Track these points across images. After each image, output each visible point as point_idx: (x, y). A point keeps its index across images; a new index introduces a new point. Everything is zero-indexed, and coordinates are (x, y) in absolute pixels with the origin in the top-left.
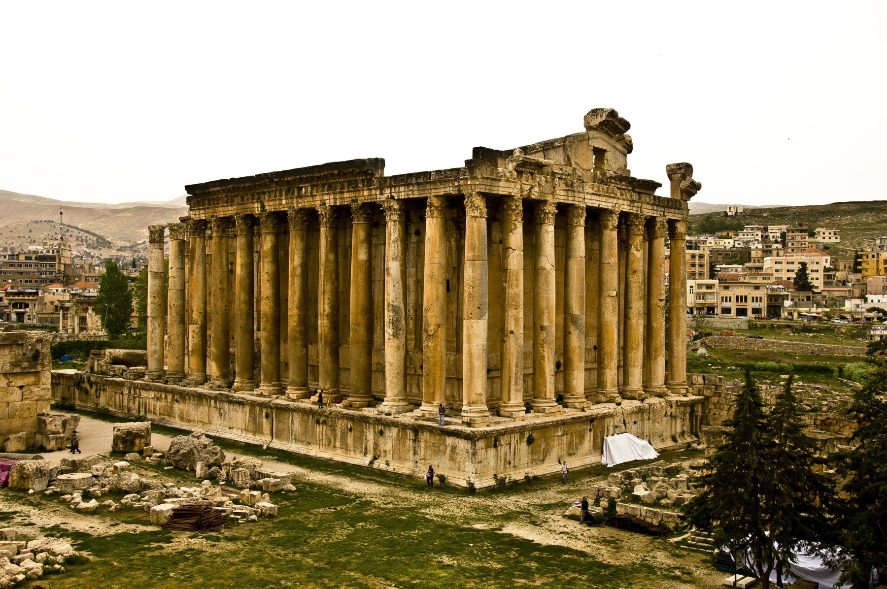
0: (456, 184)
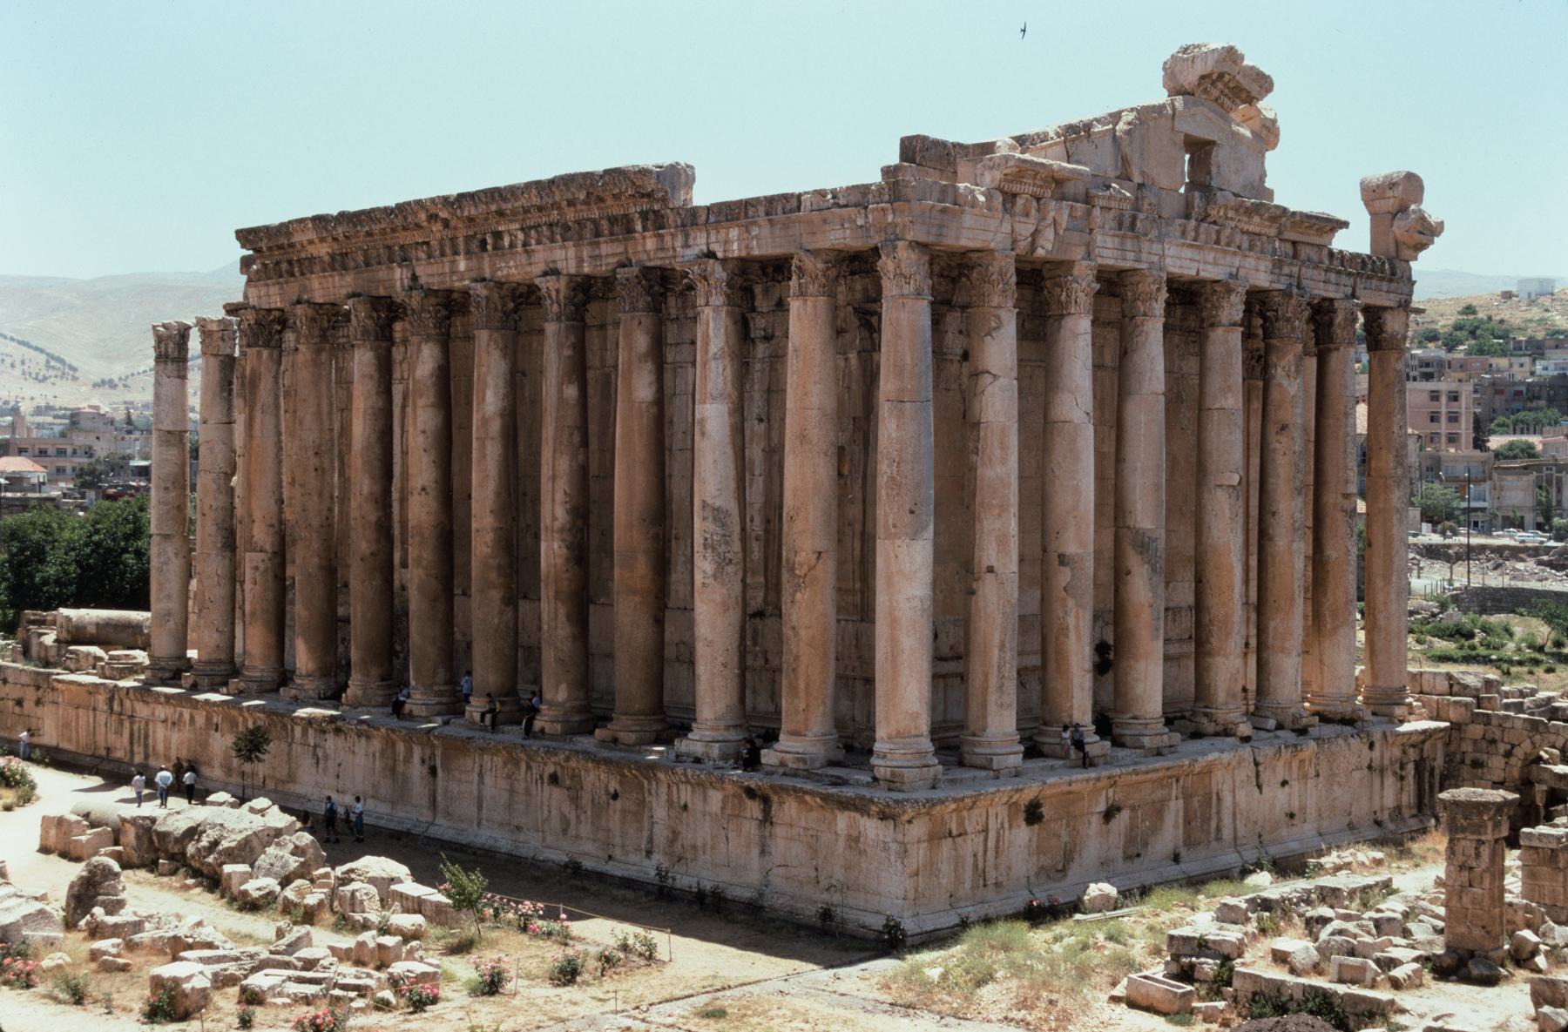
0: (860, 222)
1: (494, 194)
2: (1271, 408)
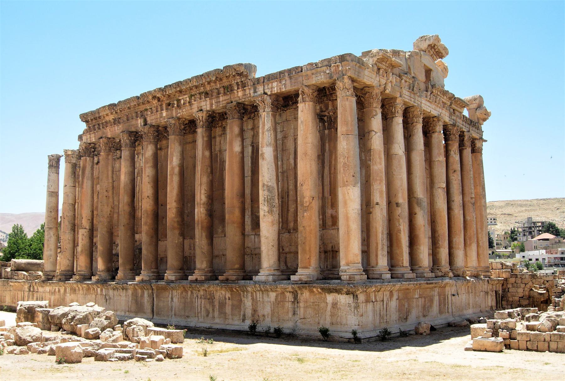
0: (328, 72)
1: (179, 84)
2: (450, 164)
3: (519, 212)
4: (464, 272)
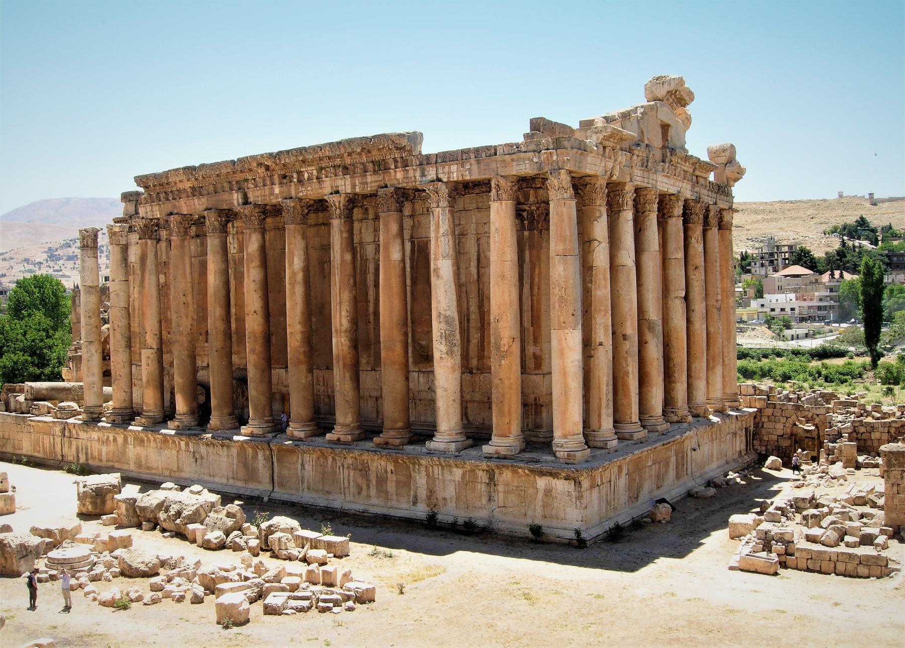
0: (535, 160)
1: (301, 151)
2: (690, 258)
3: (754, 222)
4: (706, 411)
